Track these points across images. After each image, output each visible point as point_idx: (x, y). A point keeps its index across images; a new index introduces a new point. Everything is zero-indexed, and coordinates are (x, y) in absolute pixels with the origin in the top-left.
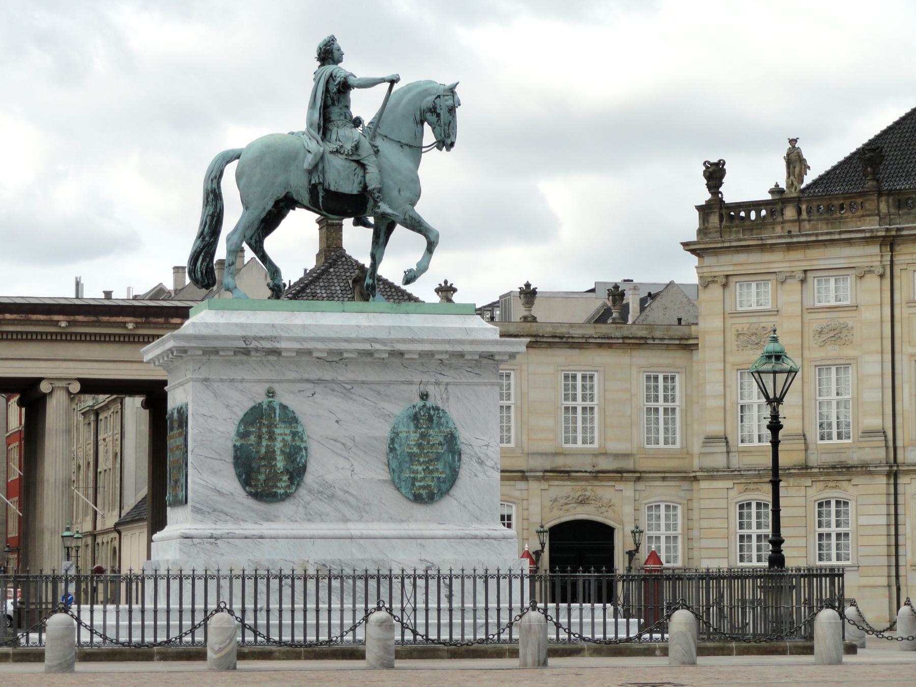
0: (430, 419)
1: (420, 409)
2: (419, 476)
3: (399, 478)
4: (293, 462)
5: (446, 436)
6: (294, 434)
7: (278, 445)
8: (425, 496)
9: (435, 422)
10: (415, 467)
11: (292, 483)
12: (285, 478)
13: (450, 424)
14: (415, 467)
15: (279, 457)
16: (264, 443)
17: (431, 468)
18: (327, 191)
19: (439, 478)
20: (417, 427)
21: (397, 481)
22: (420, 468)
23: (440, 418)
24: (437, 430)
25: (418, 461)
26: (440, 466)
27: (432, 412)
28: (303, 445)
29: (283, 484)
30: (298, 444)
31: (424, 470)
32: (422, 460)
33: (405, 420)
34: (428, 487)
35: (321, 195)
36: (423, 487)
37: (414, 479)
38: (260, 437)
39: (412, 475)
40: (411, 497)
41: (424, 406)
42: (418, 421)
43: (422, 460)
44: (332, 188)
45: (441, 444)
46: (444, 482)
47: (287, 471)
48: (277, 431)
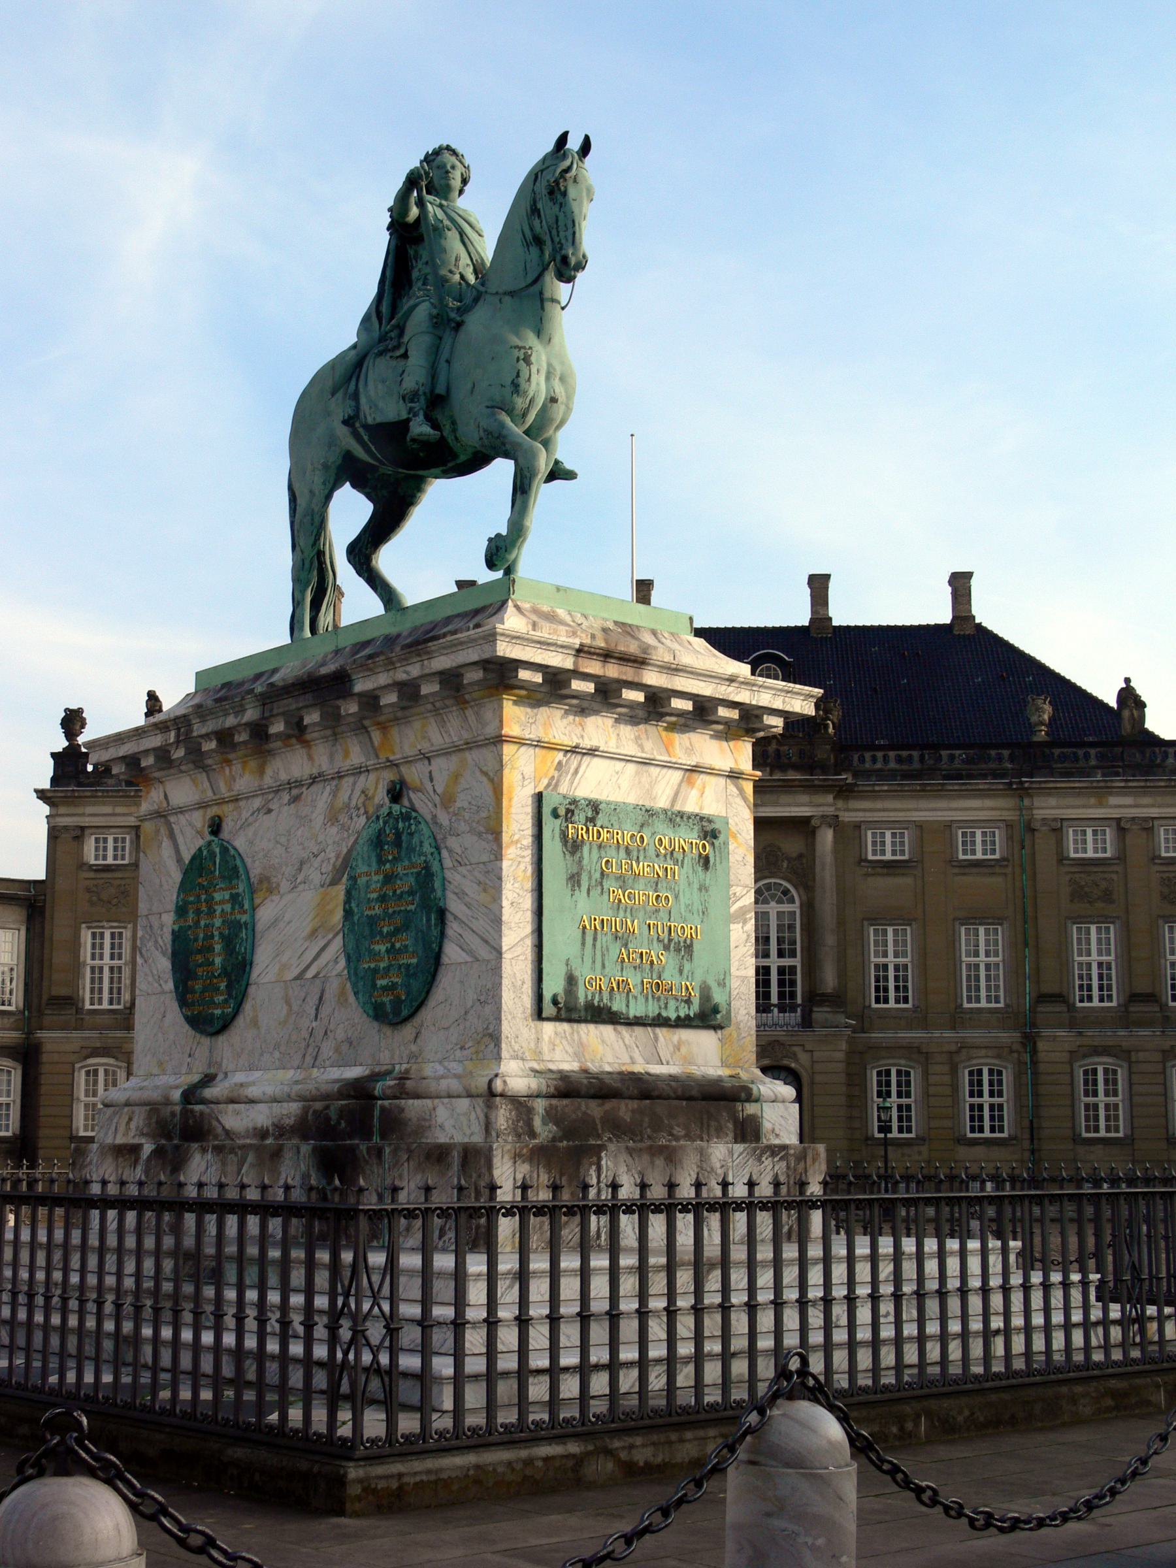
0: (398, 843)
1: (385, 823)
2: (382, 965)
3: (356, 974)
4: (231, 955)
5: (418, 874)
6: (235, 899)
7: (218, 922)
8: (389, 1008)
9: (404, 845)
10: (377, 947)
11: (230, 995)
12: (223, 986)
13: (427, 848)
14: (377, 947)
15: (218, 948)
16: (202, 923)
17: (398, 945)
18: (366, 427)
19: (408, 966)
20: (381, 861)
21: (353, 978)
22: (382, 948)
23: (411, 834)
24: (406, 863)
25: (381, 933)
26: (406, 940)
28: (244, 918)
29: (221, 998)
30: (238, 917)
31: (388, 951)
32: (385, 930)
33: (365, 849)
34: (392, 987)
35: (366, 438)
36: (385, 989)
37: (375, 971)
38: (198, 912)
39: (372, 965)
40: (371, 1012)
41: (390, 814)
42: (382, 849)
43: (385, 930)
44: (370, 421)
45: (411, 893)
46: (415, 974)
47: (225, 973)
48: (218, 896)
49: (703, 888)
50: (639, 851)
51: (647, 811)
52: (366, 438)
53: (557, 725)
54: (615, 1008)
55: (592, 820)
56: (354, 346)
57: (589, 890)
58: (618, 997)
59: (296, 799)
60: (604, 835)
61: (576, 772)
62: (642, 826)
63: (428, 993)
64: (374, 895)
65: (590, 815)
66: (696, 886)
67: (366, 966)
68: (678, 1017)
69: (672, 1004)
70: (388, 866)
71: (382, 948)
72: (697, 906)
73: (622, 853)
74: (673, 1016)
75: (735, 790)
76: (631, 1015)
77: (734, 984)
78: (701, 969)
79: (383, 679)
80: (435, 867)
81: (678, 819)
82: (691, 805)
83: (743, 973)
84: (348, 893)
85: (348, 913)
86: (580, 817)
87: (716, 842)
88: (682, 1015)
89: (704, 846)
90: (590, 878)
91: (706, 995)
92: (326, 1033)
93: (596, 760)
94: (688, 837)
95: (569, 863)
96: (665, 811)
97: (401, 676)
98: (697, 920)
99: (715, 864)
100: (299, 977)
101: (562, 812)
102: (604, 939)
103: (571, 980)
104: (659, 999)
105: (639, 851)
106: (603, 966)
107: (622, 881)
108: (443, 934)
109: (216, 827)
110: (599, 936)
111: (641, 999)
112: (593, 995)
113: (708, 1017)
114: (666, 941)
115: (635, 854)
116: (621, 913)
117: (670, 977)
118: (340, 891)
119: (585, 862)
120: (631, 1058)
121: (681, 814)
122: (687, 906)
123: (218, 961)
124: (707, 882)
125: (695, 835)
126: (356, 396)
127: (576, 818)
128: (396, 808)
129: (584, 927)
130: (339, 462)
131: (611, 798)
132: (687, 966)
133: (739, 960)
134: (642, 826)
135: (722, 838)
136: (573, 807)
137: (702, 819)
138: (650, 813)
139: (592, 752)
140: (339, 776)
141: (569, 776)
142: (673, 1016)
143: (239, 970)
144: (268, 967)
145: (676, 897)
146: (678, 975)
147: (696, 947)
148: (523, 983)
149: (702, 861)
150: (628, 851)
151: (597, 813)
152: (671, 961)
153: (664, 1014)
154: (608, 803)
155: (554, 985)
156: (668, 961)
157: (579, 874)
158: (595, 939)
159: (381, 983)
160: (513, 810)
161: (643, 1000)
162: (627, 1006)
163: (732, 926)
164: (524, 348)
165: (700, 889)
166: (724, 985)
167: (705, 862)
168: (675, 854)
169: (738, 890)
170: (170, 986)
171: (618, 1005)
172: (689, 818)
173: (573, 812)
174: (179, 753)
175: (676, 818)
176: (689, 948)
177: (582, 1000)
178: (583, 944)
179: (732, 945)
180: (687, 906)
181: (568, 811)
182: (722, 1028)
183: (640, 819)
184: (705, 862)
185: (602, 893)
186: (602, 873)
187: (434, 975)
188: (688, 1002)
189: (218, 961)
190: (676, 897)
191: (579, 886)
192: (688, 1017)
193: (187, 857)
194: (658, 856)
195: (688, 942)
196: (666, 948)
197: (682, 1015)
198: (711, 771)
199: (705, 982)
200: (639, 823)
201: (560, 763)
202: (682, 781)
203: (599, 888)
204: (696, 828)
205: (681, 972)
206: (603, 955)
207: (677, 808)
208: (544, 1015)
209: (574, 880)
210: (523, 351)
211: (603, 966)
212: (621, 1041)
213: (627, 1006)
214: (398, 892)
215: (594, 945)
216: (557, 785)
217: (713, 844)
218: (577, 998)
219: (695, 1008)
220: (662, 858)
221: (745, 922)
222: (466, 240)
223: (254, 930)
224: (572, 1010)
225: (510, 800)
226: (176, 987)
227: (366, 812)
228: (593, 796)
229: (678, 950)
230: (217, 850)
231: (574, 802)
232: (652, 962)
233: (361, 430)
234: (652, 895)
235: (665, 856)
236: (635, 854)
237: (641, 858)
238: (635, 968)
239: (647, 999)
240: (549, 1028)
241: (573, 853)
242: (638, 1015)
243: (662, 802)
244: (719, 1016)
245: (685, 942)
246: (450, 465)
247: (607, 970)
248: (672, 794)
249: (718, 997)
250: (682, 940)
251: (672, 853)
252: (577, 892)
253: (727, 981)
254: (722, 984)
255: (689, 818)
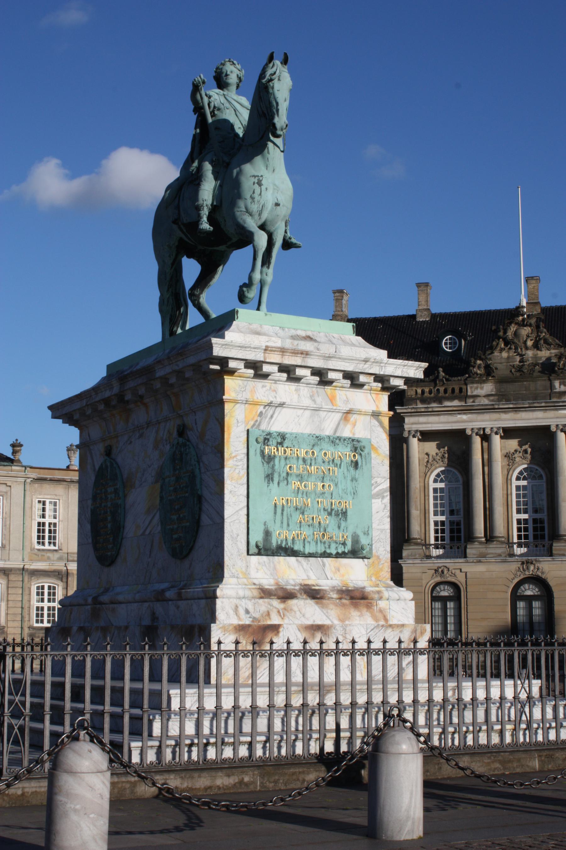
2: (175, 526)
7: (109, 504)
12: (111, 539)
15: (109, 518)
16: (103, 505)
17: (181, 516)
22: (175, 517)
27: (182, 449)
32: (176, 507)
35: (185, 230)
39: (171, 527)
41: (178, 443)
43: (176, 507)
44: (185, 221)
48: (109, 490)
49: (353, 479)
50: (311, 460)
51: (317, 437)
52: (185, 230)
53: (261, 391)
54: (296, 548)
55: (281, 444)
56: (178, 180)
57: (279, 483)
58: (298, 542)
59: (141, 436)
60: (288, 451)
61: (272, 417)
62: (314, 446)
63: (194, 542)
64: (172, 488)
65: (279, 440)
66: (349, 478)
67: (168, 527)
68: (338, 553)
69: (333, 546)
70: (177, 472)
71: (175, 517)
72: (350, 489)
73: (301, 461)
74: (334, 552)
75: (376, 423)
76: (307, 552)
77: (375, 534)
78: (353, 525)
79: (168, 370)
80: (197, 471)
81: (337, 441)
82: (346, 433)
83: (382, 527)
84: (162, 487)
85: (162, 498)
86: (273, 442)
87: (363, 454)
88: (340, 551)
89: (354, 456)
90: (280, 476)
91: (356, 540)
92: (154, 565)
93: (284, 410)
94: (345, 451)
95: (266, 469)
96: (329, 437)
97: (176, 368)
98: (350, 498)
99: (362, 466)
100: (143, 534)
101: (261, 439)
102: (289, 510)
103: (267, 534)
104: (324, 543)
105: (311, 460)
106: (288, 525)
107: (300, 478)
108: (200, 509)
109: (108, 452)
110: (285, 509)
111: (313, 544)
112: (282, 541)
113: (356, 552)
114: (329, 510)
115: (309, 462)
116: (300, 495)
117: (333, 530)
118: (158, 486)
119: (276, 467)
120: (308, 576)
121: (339, 438)
122: (343, 490)
123: (109, 525)
124: (357, 476)
125: (349, 449)
126: (178, 207)
127: (270, 443)
128: (181, 440)
129: (275, 504)
130: (177, 244)
131: (295, 431)
132: (343, 524)
133: (379, 520)
134: (314, 446)
135: (366, 451)
136: (268, 437)
137: (353, 440)
138: (319, 438)
139: (282, 405)
140: (158, 422)
141: (267, 419)
142: (334, 552)
143: (118, 529)
144: (131, 529)
145: (336, 485)
146: (337, 529)
147: (349, 513)
148: (238, 535)
149: (353, 464)
150: (304, 460)
151: (284, 440)
152: (332, 521)
153: (328, 551)
154: (291, 434)
155: (257, 537)
156: (331, 522)
157: (272, 474)
158: (283, 510)
159: (175, 536)
160: (231, 440)
161: (314, 544)
162: (304, 547)
163: (373, 501)
164: (258, 176)
165: (352, 480)
166: (368, 534)
167: (356, 465)
168: (335, 461)
169: (379, 480)
170: (90, 540)
171: (298, 547)
172: (345, 440)
173: (268, 440)
174: (89, 412)
175: (335, 441)
176: (344, 514)
177: (274, 544)
178: (275, 513)
179: (374, 511)
180: (343, 490)
181: (265, 439)
182: (369, 558)
183: (312, 442)
184: (356, 465)
185: (287, 484)
186: (288, 474)
187: (197, 532)
188: (344, 544)
189: (109, 525)
190: (336, 485)
191: (273, 480)
192: (344, 553)
193: (97, 468)
194: (324, 462)
195: (344, 510)
196: (330, 514)
197: (340, 551)
198: (360, 413)
199: (355, 533)
200: (312, 444)
201: (261, 413)
202: (341, 420)
203: (286, 482)
204: (349, 446)
205: (339, 527)
206: (288, 519)
207: (338, 434)
208: (250, 553)
209: (269, 477)
210: (257, 178)
211: (288, 525)
212: (301, 567)
213: (304, 547)
214: (182, 486)
215: (282, 514)
216: (259, 425)
217: (361, 454)
218: (271, 543)
219: (349, 547)
220: (326, 463)
221: (383, 498)
222: (238, 114)
223: (124, 508)
224: (266, 549)
225: (229, 434)
226: (93, 540)
227: (170, 442)
228: (282, 430)
229: (337, 515)
230: (109, 464)
231: (269, 434)
232: (320, 523)
233: (182, 226)
234: (320, 485)
235: (329, 462)
236: (309, 462)
237: (313, 464)
238: (309, 526)
239: (317, 543)
240: (255, 559)
241: (268, 463)
242: (311, 552)
243: (328, 431)
244: (364, 552)
245: (342, 510)
246: (229, 243)
247: (290, 527)
248: (335, 427)
249: (364, 541)
250: (340, 509)
251: (333, 460)
252: (271, 484)
253: (370, 532)
254: (367, 533)
255: (345, 440)
